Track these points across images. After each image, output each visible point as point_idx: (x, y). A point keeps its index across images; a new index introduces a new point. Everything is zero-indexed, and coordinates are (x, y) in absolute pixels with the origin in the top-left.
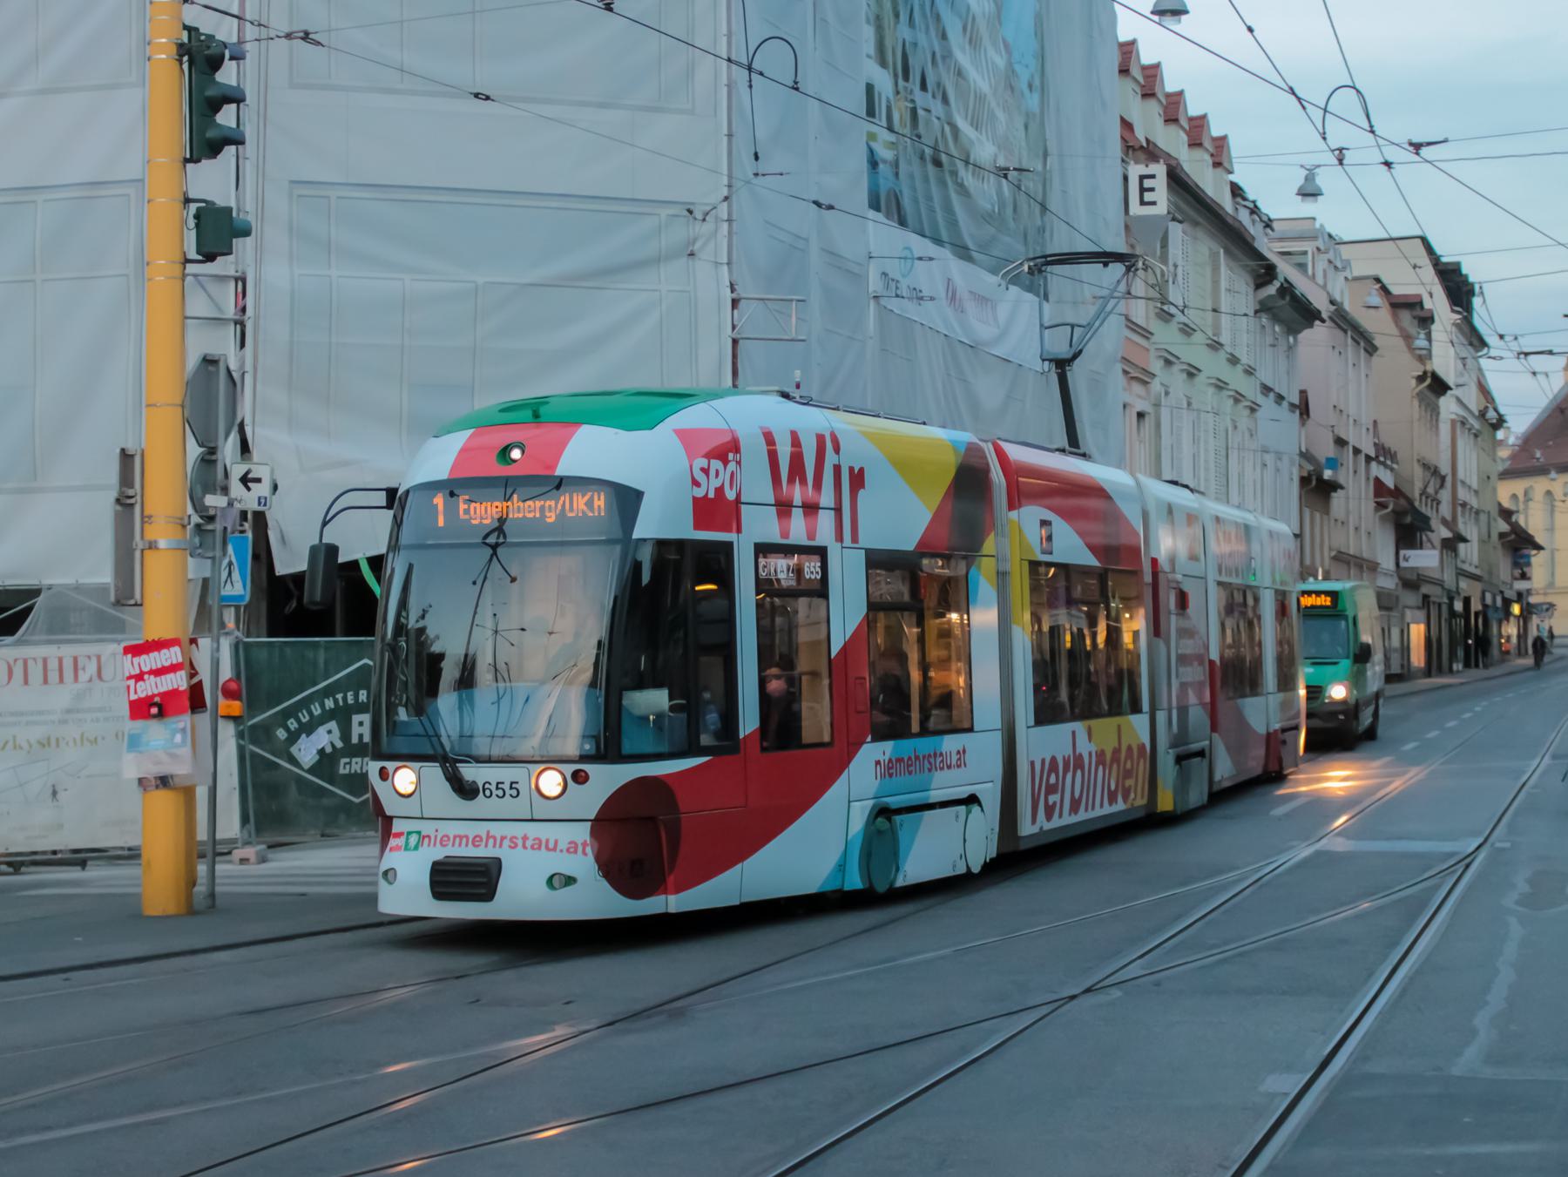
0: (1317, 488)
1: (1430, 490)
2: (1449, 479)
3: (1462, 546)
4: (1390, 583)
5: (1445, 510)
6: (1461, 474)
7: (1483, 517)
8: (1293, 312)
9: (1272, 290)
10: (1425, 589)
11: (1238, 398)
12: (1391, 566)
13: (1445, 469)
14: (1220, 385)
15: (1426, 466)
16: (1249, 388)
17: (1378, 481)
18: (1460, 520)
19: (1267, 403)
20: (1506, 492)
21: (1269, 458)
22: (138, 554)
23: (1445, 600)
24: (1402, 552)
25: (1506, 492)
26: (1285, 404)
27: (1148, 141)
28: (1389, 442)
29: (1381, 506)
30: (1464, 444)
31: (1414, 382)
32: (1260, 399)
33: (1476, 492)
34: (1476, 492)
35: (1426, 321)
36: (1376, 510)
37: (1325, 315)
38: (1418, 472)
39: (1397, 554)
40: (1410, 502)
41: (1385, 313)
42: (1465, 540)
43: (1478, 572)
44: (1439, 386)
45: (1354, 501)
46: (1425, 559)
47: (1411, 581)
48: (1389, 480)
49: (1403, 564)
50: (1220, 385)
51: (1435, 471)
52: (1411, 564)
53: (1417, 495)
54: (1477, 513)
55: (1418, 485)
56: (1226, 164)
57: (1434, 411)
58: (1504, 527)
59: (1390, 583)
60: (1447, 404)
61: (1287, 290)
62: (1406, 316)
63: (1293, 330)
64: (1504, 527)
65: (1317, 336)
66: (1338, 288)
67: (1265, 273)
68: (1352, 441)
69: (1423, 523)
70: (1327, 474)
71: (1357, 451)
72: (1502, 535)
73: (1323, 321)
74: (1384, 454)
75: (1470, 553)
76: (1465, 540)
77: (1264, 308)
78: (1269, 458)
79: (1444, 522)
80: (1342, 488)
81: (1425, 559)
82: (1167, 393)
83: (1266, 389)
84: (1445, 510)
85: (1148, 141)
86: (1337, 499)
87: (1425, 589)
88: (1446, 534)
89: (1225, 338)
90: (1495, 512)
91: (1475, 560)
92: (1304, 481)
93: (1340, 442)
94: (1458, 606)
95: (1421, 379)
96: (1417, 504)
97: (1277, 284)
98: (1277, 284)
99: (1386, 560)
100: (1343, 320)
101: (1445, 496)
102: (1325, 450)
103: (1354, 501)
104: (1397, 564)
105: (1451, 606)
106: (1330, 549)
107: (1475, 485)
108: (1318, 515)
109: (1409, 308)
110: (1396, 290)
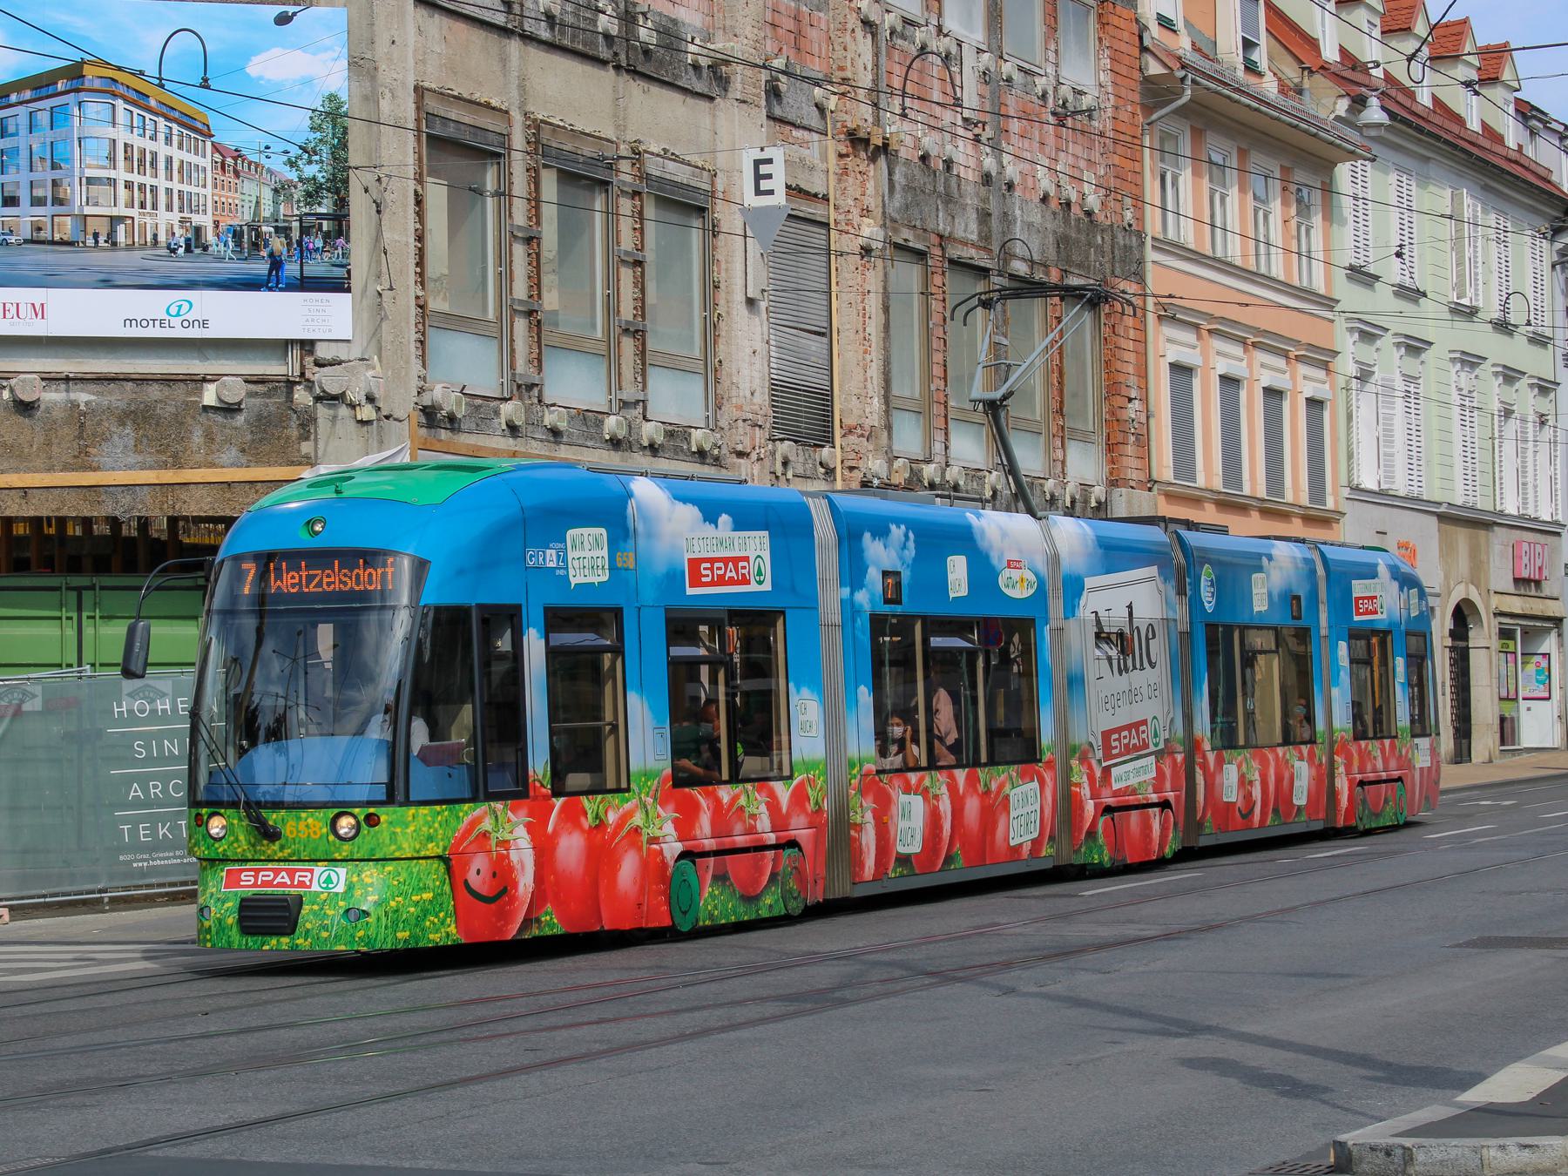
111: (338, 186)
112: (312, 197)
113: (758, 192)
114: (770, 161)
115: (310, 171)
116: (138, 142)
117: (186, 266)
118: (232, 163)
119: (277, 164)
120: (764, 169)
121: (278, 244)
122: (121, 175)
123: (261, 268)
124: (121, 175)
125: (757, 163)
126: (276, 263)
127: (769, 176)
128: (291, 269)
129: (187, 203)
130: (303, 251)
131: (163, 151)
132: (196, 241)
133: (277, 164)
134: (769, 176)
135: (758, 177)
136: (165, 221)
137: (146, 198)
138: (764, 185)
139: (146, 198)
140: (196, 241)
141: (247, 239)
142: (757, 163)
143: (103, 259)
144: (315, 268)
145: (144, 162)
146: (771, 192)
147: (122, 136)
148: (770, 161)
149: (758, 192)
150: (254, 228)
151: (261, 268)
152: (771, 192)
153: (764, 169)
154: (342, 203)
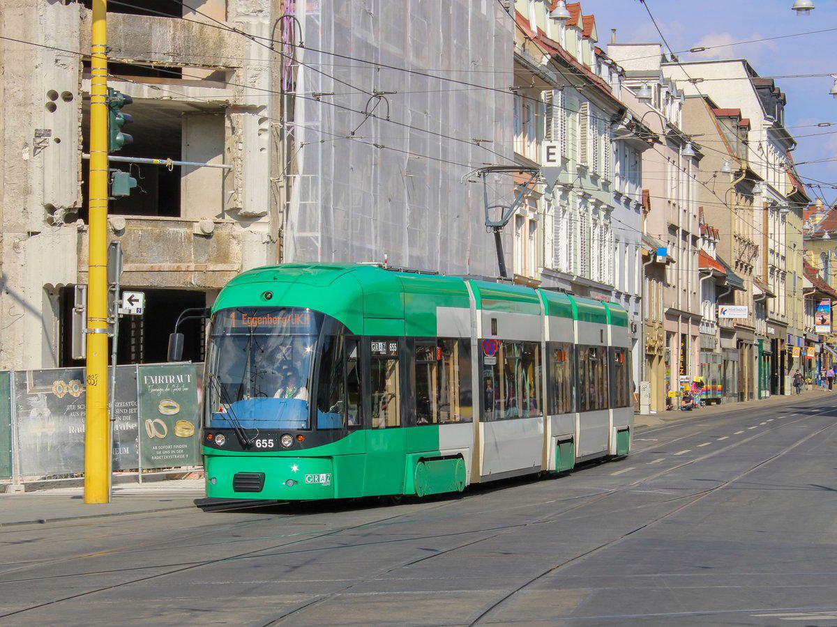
1: (745, 259)
2: (761, 248)
3: (770, 300)
5: (758, 270)
6: (771, 246)
7: (789, 277)
12: (713, 318)
13: (758, 240)
15: (740, 239)
17: (703, 255)
18: (770, 281)
22: (84, 335)
23: (755, 342)
24: (720, 307)
26: (632, 204)
27: (539, 29)
29: (703, 273)
31: (732, 177)
32: (613, 203)
33: (783, 258)
34: (783, 258)
36: (701, 276)
37: (662, 139)
39: (717, 308)
42: (773, 296)
43: (785, 320)
46: (739, 312)
48: (711, 252)
49: (721, 316)
51: (749, 244)
52: (727, 315)
53: (734, 264)
54: (784, 274)
56: (593, 36)
58: (807, 284)
60: (762, 195)
61: (636, 125)
62: (728, 124)
64: (807, 284)
66: (673, 112)
67: (621, 111)
68: (682, 226)
70: (659, 259)
71: (685, 234)
72: (806, 290)
73: (661, 143)
74: (709, 233)
76: (773, 296)
79: (756, 282)
80: (674, 262)
81: (739, 312)
82: (549, 205)
83: (618, 196)
85: (539, 29)
86: (670, 271)
88: (759, 292)
89: (590, 163)
90: (800, 270)
91: (782, 311)
93: (673, 229)
94: (767, 347)
95: (738, 174)
96: (733, 269)
97: (626, 121)
98: (626, 121)
100: (676, 139)
101: (757, 264)
104: (717, 316)
105: (760, 346)
106: (664, 307)
107: (782, 253)
108: (654, 282)
110: (722, 104)
113: (549, 160)
114: (554, 147)
120: (551, 151)
125: (549, 148)
127: (554, 154)
134: (554, 154)
135: (549, 154)
138: (551, 157)
142: (549, 148)
146: (554, 161)
148: (554, 147)
149: (549, 160)
152: (554, 161)
153: (551, 151)
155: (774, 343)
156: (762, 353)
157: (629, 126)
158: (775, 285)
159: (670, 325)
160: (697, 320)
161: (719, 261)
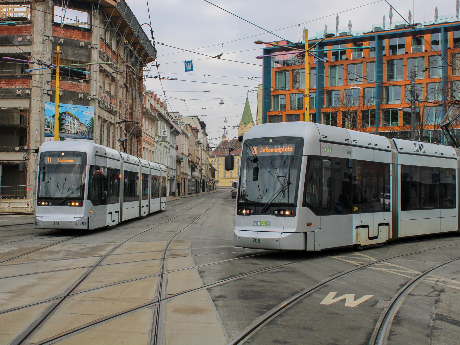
0: (179, 162)
4: (190, 177)
8: (175, 133)
9: (173, 130)
10: (196, 178)
11: (167, 148)
13: (200, 157)
14: (164, 146)
16: (169, 146)
19: (171, 148)
20: (210, 160)
21: (172, 158)
25: (210, 160)
28: (191, 153)
29: (189, 164)
30: (203, 152)
35: (197, 132)
38: (195, 158)
40: (194, 163)
41: (190, 130)
44: (199, 143)
45: (185, 163)
47: (194, 177)
50: (164, 146)
55: (195, 160)
57: (198, 147)
59: (190, 177)
62: (194, 131)
63: (175, 136)
65: (179, 137)
66: (183, 128)
67: (172, 127)
68: (185, 154)
69: (196, 167)
75: (204, 172)
77: (171, 133)
78: (172, 158)
79: (200, 167)
81: (196, 173)
83: (171, 146)
84: (200, 165)
86: (182, 164)
87: (196, 178)
88: (200, 169)
92: (177, 161)
93: (183, 154)
94: (202, 181)
99: (190, 174)
100: (183, 133)
101: (200, 162)
102: (181, 156)
103: (185, 163)
109: (195, 131)
111: (92, 127)
112: (90, 129)
115: (90, 125)
116: (72, 121)
117: (76, 136)
118: (81, 124)
119: (86, 124)
121: (86, 134)
122: (70, 125)
123: (84, 136)
124: (70, 125)
126: (86, 136)
128: (87, 137)
129: (77, 129)
130: (89, 135)
131: (74, 122)
132: (77, 133)
133: (86, 124)
136: (74, 130)
137: (72, 128)
139: (72, 128)
140: (77, 133)
141: (83, 133)
143: (68, 135)
144: (90, 137)
145: (72, 124)
147: (70, 121)
150: (83, 132)
151: (84, 136)
154: (93, 129)
155: (203, 180)
156: (201, 182)
157: (174, 131)
158: (203, 167)
159: (182, 176)
160: (187, 175)
161: (192, 162)
